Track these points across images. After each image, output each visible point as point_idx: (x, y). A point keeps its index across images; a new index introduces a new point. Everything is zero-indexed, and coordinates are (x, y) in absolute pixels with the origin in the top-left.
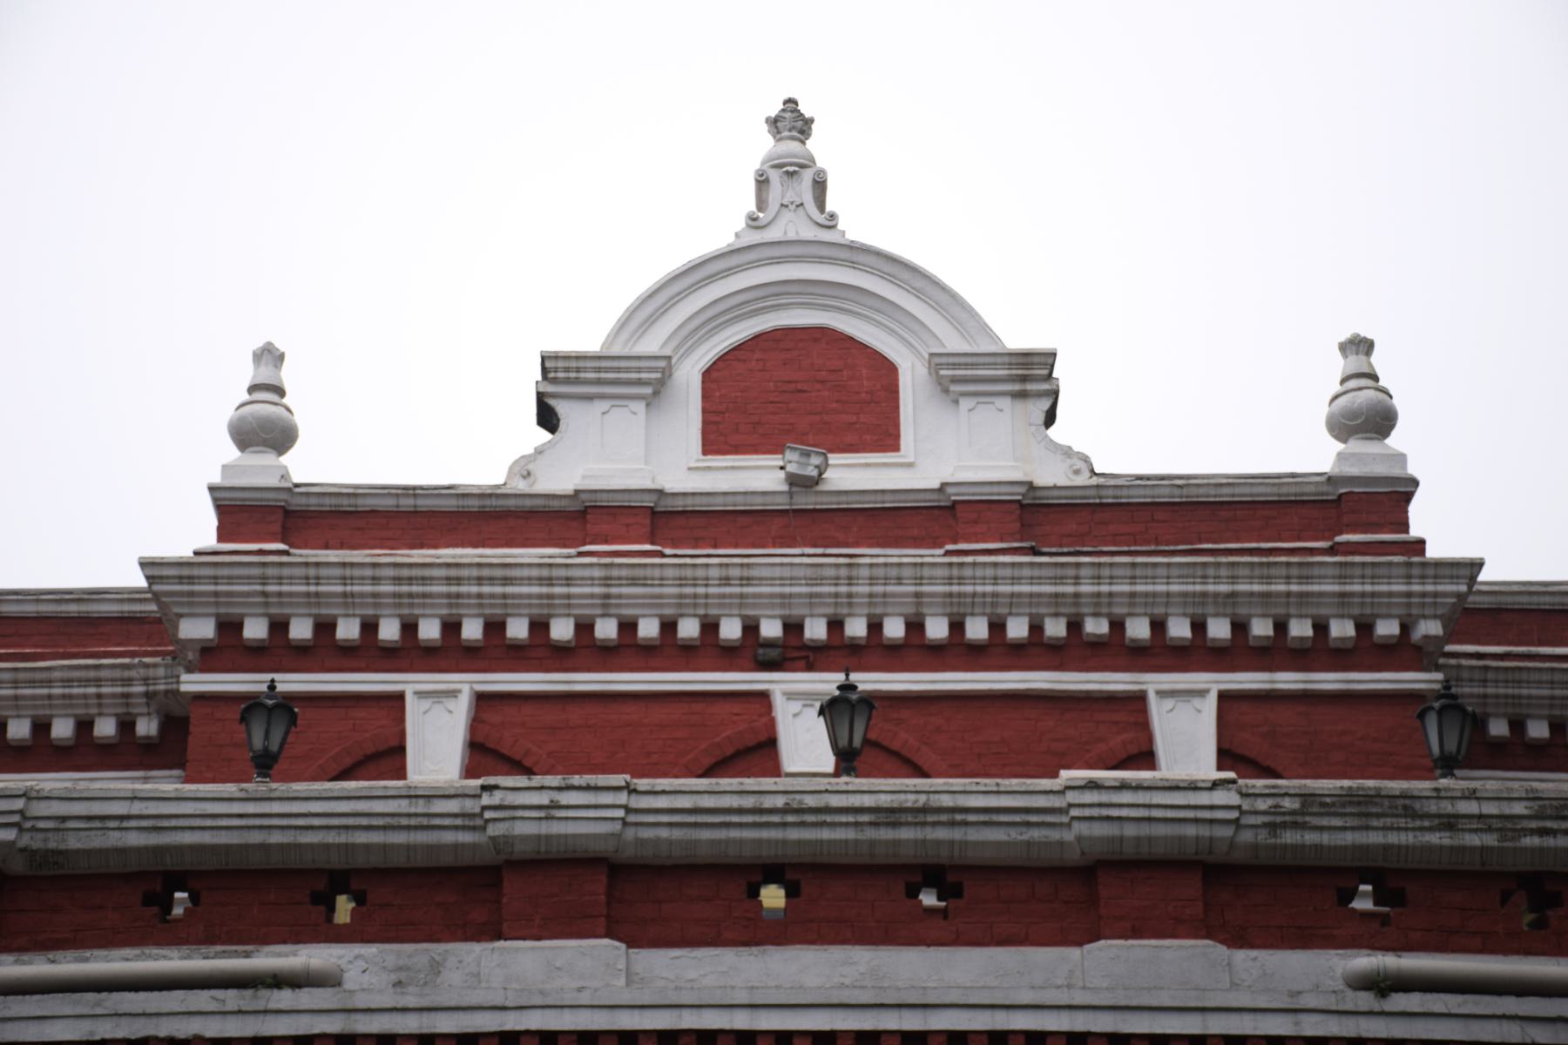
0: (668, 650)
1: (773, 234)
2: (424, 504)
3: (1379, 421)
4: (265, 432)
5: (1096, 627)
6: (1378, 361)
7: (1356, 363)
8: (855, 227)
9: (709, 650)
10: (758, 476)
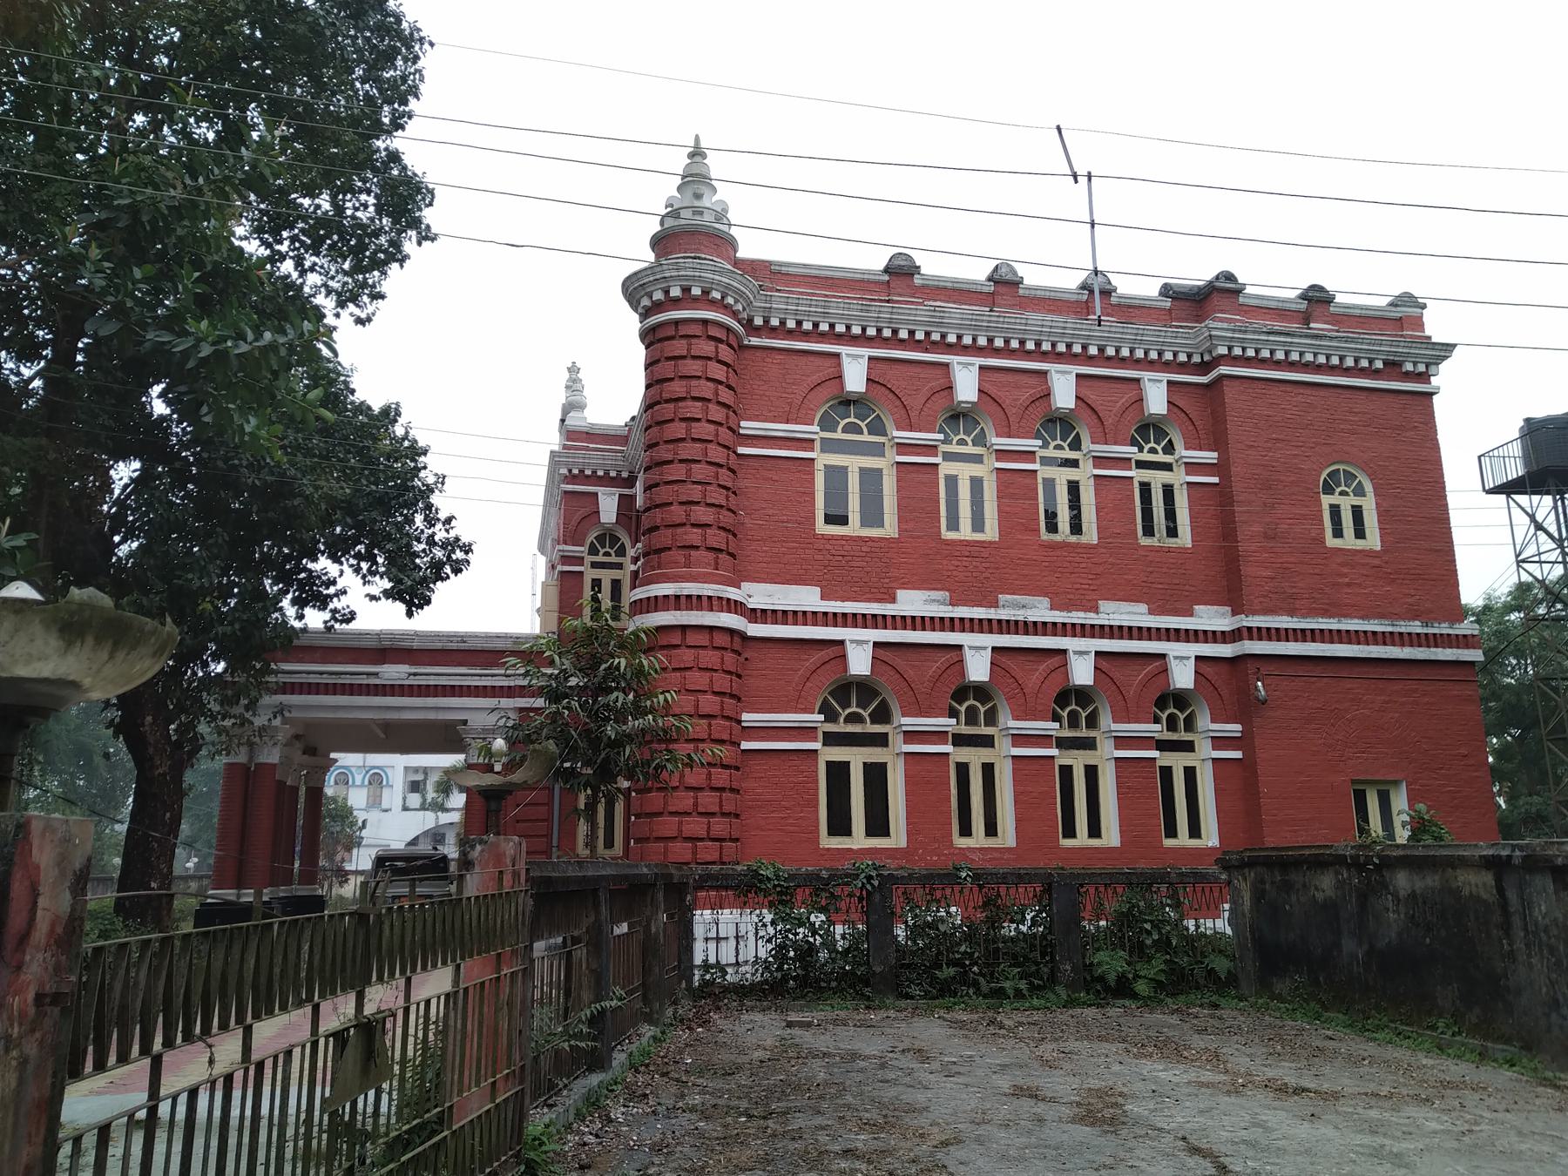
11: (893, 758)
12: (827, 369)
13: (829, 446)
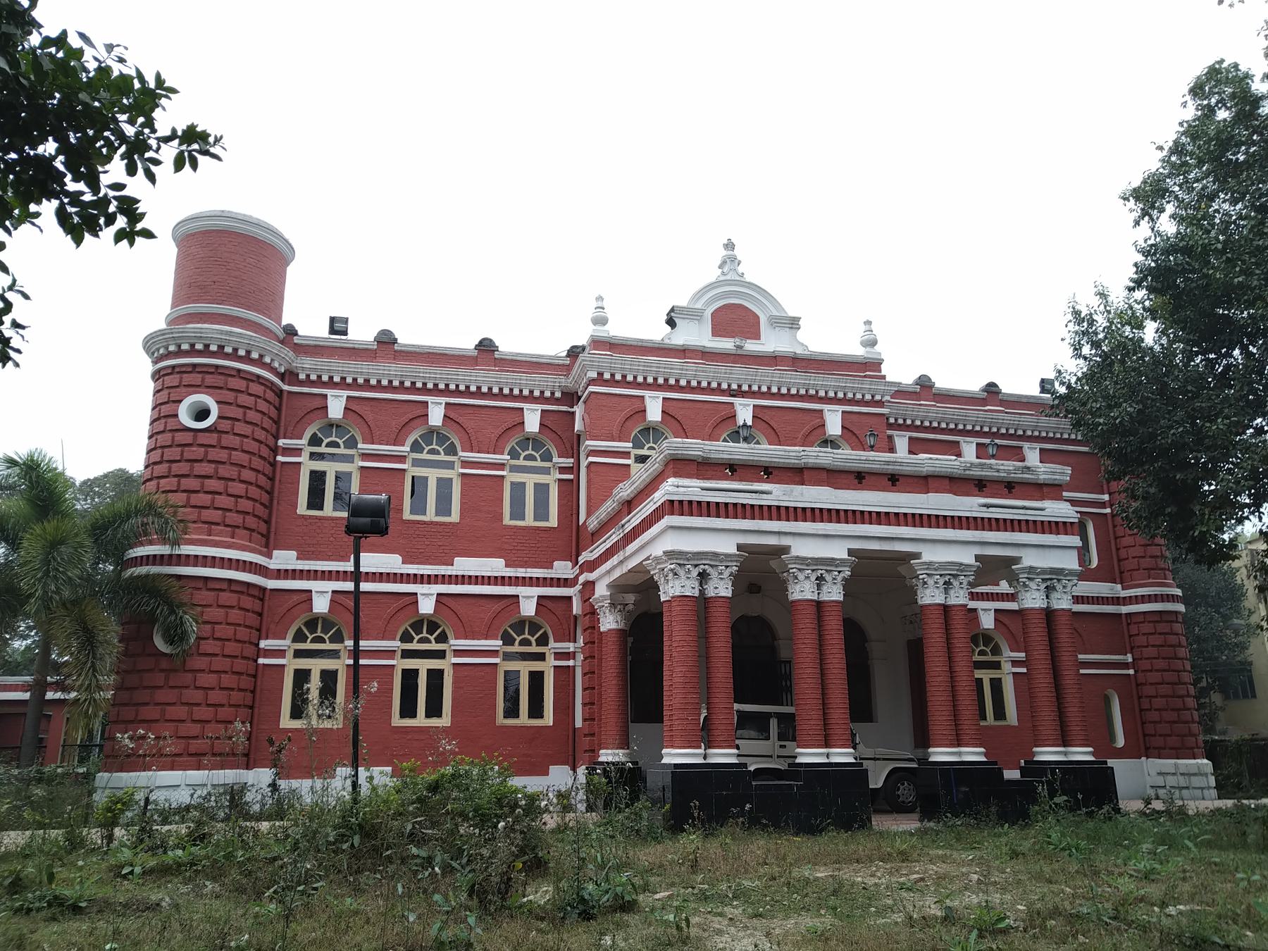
0: (709, 390)
1: (728, 277)
3: (873, 343)
5: (812, 392)
6: (873, 327)
7: (867, 327)
8: (748, 278)
9: (719, 391)
10: (727, 344)
11: (548, 667)
12: (512, 419)
13: (515, 469)
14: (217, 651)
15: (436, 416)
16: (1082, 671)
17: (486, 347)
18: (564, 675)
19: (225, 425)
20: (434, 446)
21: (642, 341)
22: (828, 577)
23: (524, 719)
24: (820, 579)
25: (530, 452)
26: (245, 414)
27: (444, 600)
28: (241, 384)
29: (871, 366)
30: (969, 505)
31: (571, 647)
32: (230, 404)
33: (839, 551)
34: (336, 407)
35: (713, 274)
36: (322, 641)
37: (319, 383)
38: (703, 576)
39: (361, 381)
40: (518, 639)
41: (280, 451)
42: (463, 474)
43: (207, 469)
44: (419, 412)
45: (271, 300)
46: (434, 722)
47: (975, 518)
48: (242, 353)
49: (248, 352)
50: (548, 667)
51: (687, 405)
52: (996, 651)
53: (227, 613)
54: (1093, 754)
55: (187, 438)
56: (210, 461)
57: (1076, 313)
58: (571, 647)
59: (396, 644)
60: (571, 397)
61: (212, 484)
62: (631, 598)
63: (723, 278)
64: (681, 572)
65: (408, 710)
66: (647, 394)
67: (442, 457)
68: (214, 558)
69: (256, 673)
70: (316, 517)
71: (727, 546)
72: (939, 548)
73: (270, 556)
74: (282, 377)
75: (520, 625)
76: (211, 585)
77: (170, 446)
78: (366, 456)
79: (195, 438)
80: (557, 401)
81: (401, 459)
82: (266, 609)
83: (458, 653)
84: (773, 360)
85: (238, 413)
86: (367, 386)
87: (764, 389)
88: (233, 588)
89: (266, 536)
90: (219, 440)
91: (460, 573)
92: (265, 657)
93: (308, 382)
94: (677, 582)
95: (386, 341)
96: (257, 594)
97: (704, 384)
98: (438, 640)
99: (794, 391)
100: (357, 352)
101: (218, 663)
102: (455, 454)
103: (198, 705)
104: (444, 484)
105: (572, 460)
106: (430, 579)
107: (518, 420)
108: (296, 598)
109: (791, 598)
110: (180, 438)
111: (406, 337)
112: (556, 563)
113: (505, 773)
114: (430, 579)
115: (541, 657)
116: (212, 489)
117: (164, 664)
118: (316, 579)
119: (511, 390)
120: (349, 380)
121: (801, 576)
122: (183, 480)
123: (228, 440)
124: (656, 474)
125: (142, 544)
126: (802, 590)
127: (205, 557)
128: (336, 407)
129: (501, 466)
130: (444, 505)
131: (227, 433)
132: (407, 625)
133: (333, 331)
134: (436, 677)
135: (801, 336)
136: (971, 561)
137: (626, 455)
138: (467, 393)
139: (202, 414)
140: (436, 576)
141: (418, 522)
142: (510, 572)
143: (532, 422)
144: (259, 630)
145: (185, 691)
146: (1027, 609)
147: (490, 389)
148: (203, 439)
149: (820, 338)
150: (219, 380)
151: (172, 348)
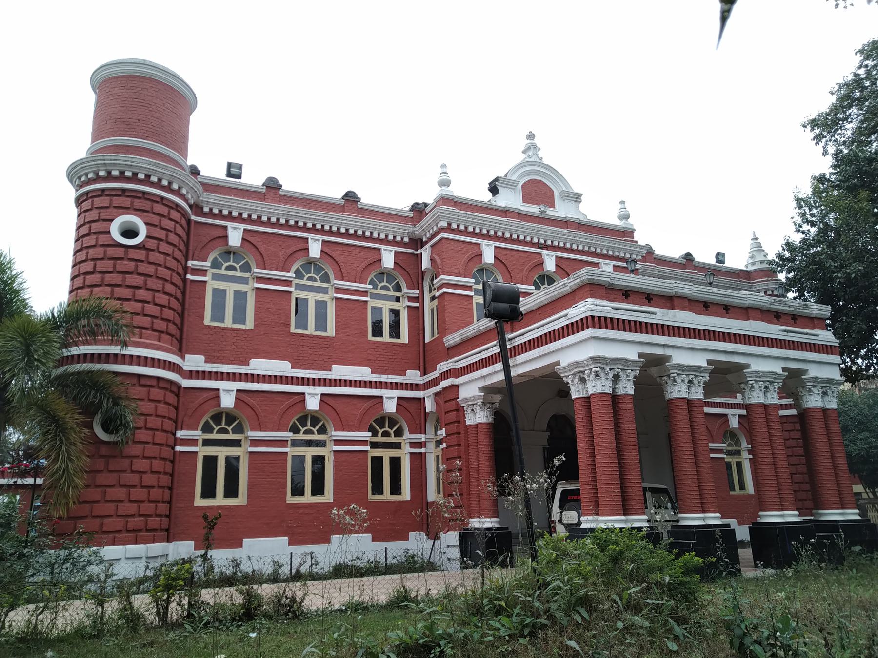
0: (524, 243)
2: (478, 204)
3: (626, 217)
4: (445, 183)
5: (593, 249)
6: (626, 205)
7: (622, 206)
8: (545, 161)
10: (533, 209)
11: (405, 454)
12: (371, 257)
13: (375, 296)
14: (150, 439)
15: (315, 250)
16: (712, 455)
17: (351, 198)
18: (418, 461)
19: (152, 244)
20: (312, 275)
21: (476, 201)
22: (695, 381)
23: (387, 495)
24: (690, 382)
25: (385, 283)
26: (167, 236)
27: (326, 399)
28: (163, 210)
29: (627, 234)
30: (774, 330)
31: (422, 438)
32: (155, 226)
33: (700, 360)
34: (235, 237)
35: (521, 157)
36: (225, 431)
37: (220, 216)
38: (616, 378)
39: (254, 217)
40: (381, 431)
41: (189, 270)
42: (337, 298)
43: (138, 280)
44: (301, 246)
45: (180, 142)
46: (318, 499)
47: (780, 340)
48: (165, 183)
49: (170, 183)
50: (405, 454)
51: (510, 252)
52: (738, 443)
53: (156, 407)
54: (860, 515)
55: (120, 252)
56: (139, 274)
57: (798, 200)
58: (422, 438)
59: (288, 435)
60: (417, 243)
61: (142, 294)
62: (498, 398)
63: (529, 160)
64: (602, 374)
65: (209, 491)
66: (483, 242)
67: (319, 284)
68: (146, 358)
69: (175, 458)
70: (220, 328)
71: (631, 354)
72: (761, 361)
73: (183, 358)
74: (190, 206)
75: (381, 421)
76: (143, 382)
77: (102, 259)
78: (260, 279)
79: (126, 253)
80: (405, 245)
81: (288, 283)
82: (183, 404)
83: (338, 442)
84: (565, 223)
85: (162, 234)
86: (259, 221)
87: (562, 245)
88: (161, 385)
89: (180, 341)
90: (147, 256)
91: (338, 378)
92: (181, 445)
93: (211, 214)
94: (598, 383)
95: (273, 186)
96: (175, 389)
97: (522, 238)
98: (320, 432)
99: (581, 248)
100: (247, 193)
101: (151, 450)
102: (328, 282)
103: (134, 486)
104: (321, 306)
105: (418, 292)
106: (314, 382)
107: (377, 258)
108: (205, 395)
109: (668, 396)
110: (111, 252)
111: (289, 185)
112: (408, 372)
113: (717, 540)
114: (314, 382)
115: (398, 446)
116: (142, 298)
117: (104, 451)
118: (222, 380)
119: (372, 233)
120: (245, 216)
121: (679, 380)
122: (116, 289)
123: (155, 257)
124: (558, 297)
125: (76, 344)
126: (678, 391)
127: (139, 357)
128: (235, 237)
129: (365, 293)
130: (321, 323)
131: (153, 250)
132: (294, 419)
133: (229, 174)
134: (319, 461)
135: (582, 207)
136: (780, 371)
137: (469, 288)
138: (338, 234)
139: (130, 232)
140: (319, 379)
141: (303, 335)
142: (375, 378)
143: (388, 260)
144: (176, 422)
145: (123, 475)
146: (811, 408)
147: (356, 231)
148: (133, 254)
149: (598, 210)
150: (146, 205)
151: (91, 176)
